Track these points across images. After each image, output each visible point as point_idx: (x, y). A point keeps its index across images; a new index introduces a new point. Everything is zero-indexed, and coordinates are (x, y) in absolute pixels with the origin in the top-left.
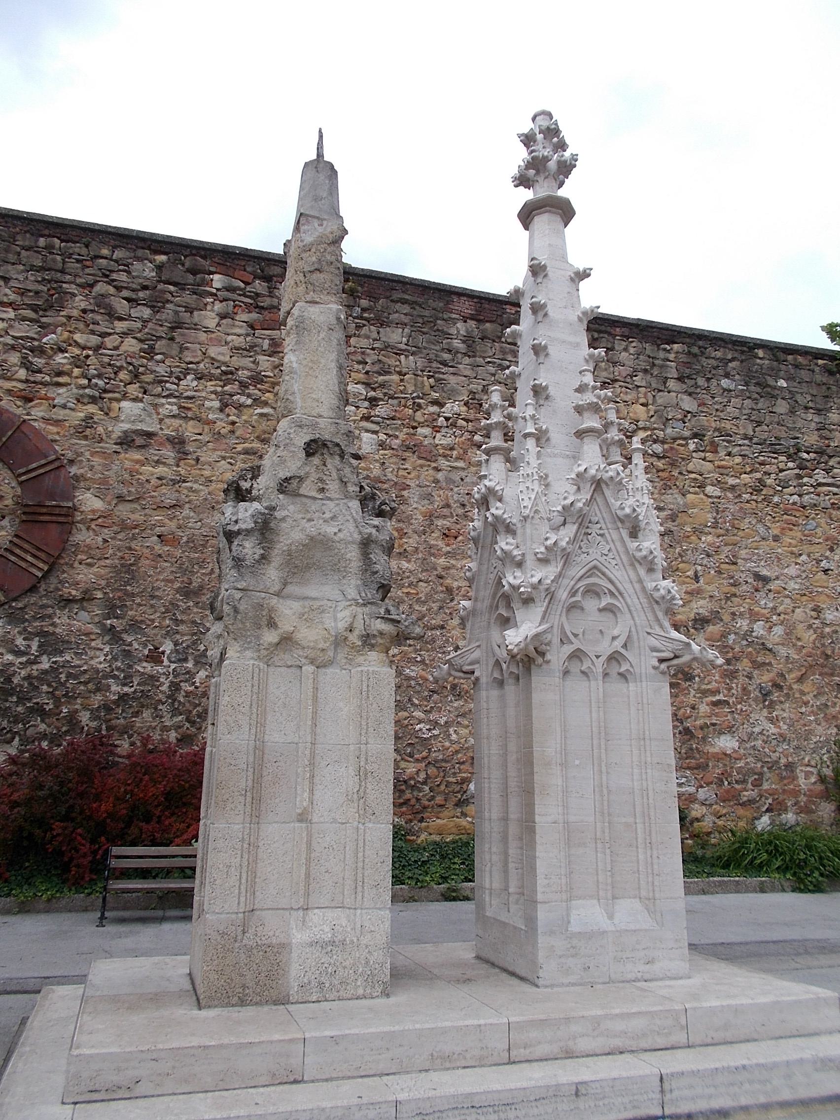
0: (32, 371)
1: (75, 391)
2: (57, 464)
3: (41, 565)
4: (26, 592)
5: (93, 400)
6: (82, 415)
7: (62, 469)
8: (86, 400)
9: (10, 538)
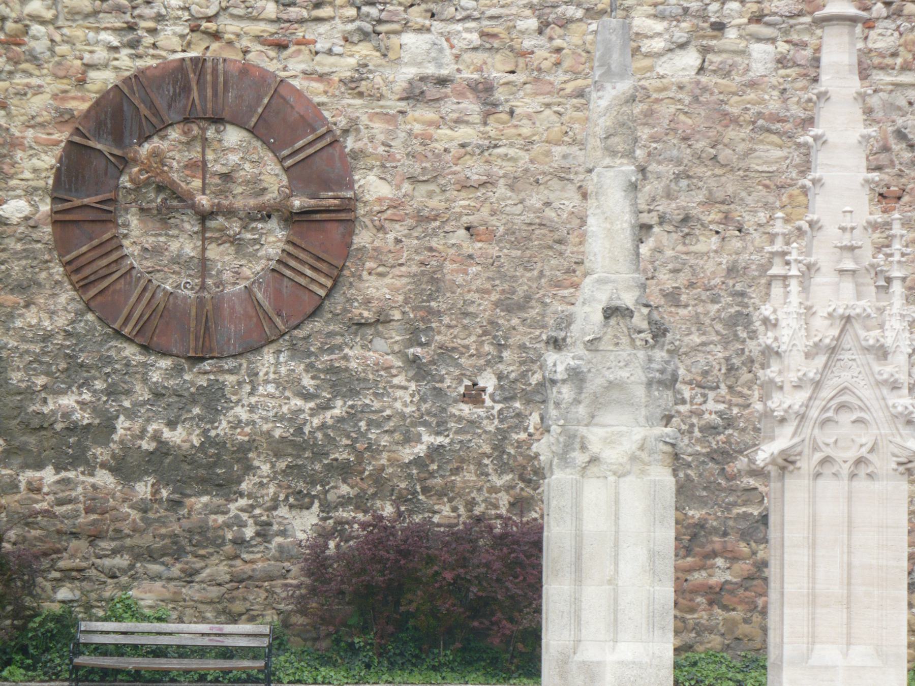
0: (284, 5)
1: (341, 27)
2: (328, 139)
3: (323, 280)
4: (309, 317)
5: (365, 36)
6: (352, 61)
7: (335, 144)
8: (355, 39)
9: (281, 245)
